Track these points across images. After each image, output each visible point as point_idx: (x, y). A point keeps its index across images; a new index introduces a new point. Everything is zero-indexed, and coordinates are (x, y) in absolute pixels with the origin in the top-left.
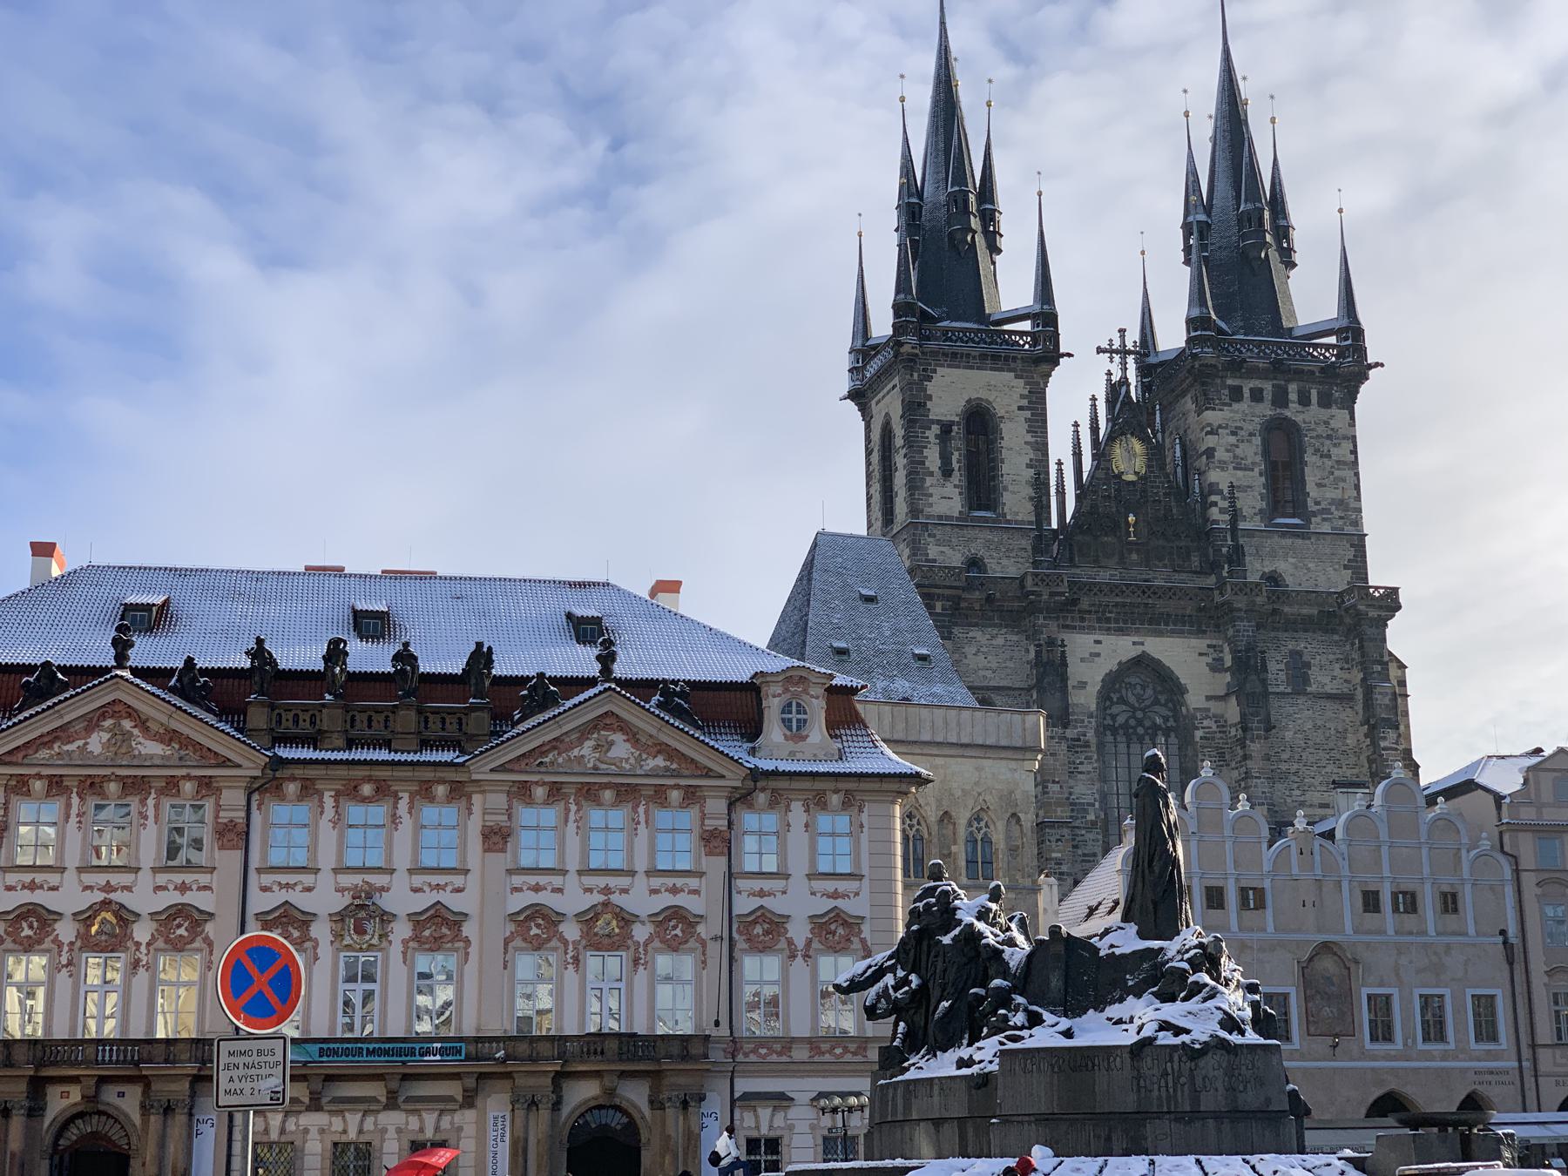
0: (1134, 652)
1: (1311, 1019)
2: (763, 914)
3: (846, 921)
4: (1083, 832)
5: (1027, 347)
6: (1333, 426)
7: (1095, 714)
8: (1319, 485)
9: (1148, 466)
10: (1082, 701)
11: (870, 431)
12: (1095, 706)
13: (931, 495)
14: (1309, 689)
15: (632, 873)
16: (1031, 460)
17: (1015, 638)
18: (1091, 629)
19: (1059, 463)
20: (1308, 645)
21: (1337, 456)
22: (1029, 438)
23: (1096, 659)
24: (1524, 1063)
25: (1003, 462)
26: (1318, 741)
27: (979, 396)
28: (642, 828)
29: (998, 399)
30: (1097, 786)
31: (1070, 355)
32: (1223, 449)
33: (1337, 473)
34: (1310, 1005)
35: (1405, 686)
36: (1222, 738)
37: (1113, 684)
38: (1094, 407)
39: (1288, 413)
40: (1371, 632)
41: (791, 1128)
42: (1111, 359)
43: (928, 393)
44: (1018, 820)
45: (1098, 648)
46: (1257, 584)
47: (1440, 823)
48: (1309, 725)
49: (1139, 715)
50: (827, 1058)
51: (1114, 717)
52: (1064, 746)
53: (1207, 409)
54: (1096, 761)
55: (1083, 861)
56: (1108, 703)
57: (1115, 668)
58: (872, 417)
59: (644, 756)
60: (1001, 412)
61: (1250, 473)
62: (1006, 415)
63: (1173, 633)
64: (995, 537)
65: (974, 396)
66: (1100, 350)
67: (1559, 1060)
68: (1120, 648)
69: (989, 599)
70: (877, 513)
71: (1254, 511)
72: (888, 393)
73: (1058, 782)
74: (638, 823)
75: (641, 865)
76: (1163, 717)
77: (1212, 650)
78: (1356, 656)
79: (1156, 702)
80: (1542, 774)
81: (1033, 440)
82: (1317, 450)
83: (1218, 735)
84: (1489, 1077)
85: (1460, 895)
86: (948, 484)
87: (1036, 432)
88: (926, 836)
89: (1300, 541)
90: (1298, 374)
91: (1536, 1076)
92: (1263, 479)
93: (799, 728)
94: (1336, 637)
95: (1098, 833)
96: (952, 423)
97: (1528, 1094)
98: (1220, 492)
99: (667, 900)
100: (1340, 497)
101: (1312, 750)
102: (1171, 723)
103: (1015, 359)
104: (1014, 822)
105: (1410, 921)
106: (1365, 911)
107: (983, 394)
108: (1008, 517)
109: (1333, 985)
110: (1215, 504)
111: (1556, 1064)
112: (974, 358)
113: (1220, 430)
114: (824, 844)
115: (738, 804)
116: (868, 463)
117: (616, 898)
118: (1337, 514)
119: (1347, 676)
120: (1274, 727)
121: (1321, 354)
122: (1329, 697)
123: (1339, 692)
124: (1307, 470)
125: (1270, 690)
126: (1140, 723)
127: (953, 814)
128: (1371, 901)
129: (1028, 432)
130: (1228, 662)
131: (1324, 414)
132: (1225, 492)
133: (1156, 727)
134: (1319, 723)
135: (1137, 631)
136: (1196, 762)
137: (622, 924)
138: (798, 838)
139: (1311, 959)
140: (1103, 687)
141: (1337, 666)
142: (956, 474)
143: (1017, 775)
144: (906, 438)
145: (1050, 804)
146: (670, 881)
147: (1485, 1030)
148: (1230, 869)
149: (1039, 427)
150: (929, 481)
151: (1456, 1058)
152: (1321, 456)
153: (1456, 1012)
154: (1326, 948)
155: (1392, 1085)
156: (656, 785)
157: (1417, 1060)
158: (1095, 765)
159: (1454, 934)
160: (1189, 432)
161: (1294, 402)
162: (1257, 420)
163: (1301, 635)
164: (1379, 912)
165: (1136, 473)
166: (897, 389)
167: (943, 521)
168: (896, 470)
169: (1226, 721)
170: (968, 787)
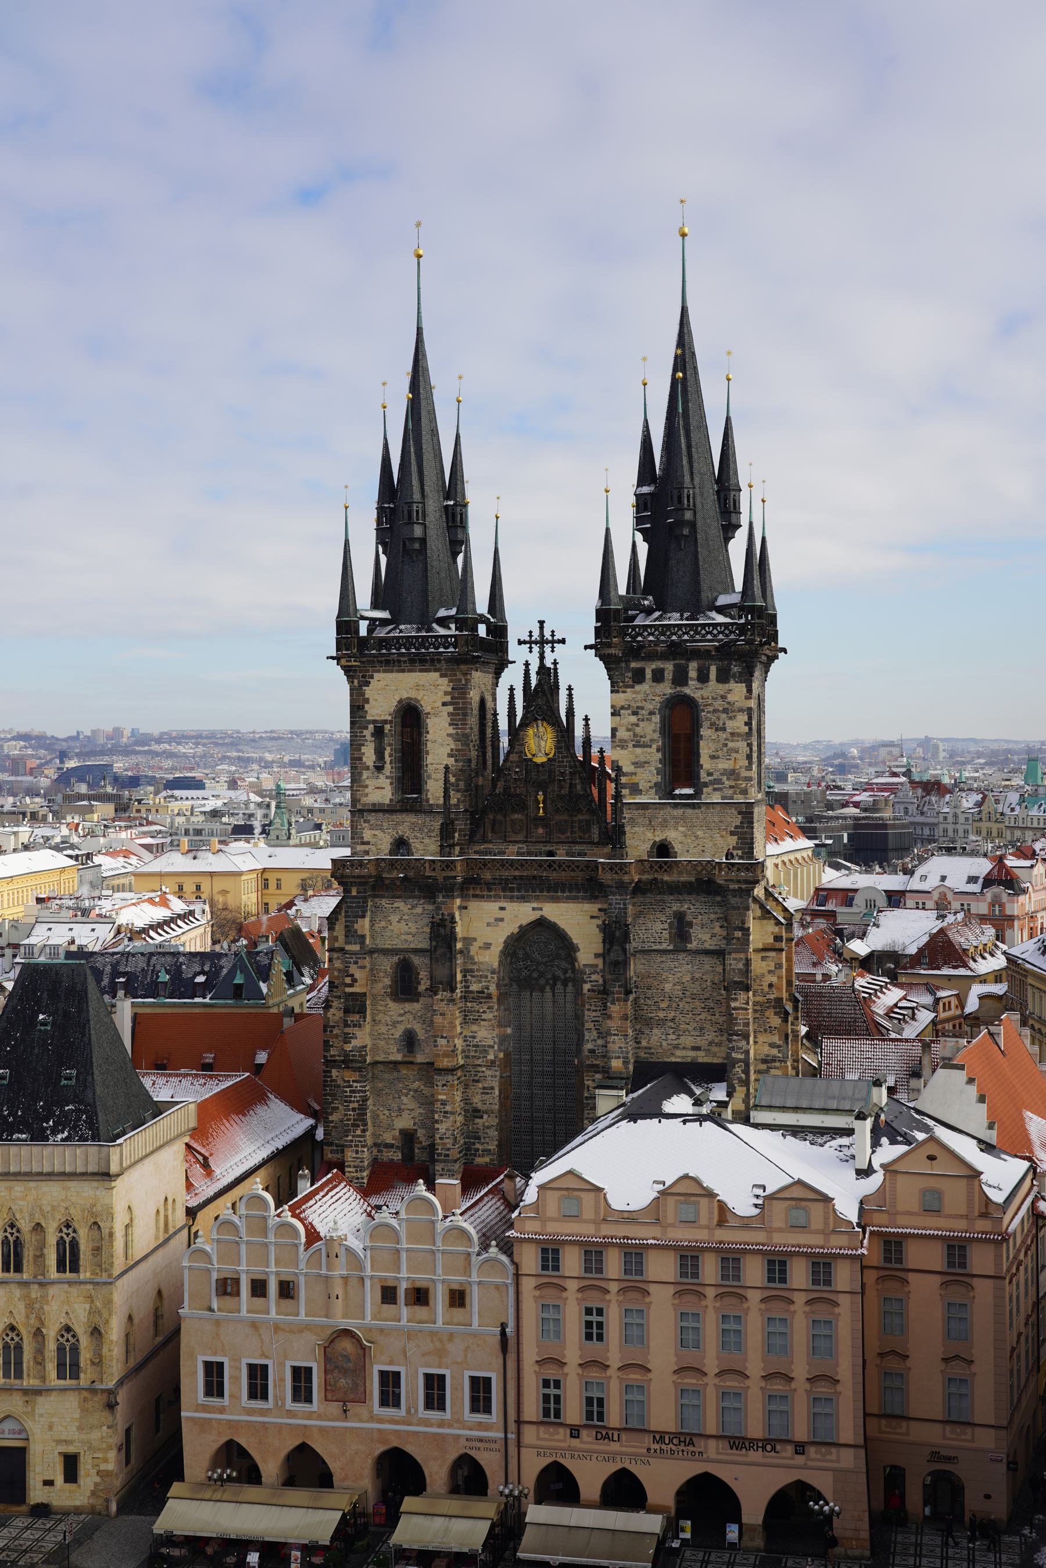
0: (534, 916)
1: (329, 1388)
4: (484, 1069)
8: (713, 757)
10: (487, 959)
13: (367, 786)
14: (689, 946)
16: (452, 750)
18: (497, 898)
20: (690, 907)
22: (451, 730)
23: (500, 923)
24: (509, 1436)
25: (427, 753)
26: (695, 991)
30: (497, 1031)
32: (624, 728)
33: (731, 745)
39: (687, 691)
42: (531, 648)
44: (99, 1227)
48: (688, 978)
57: (516, 930)
60: (427, 709)
61: (648, 750)
62: (432, 712)
63: (568, 899)
65: (405, 696)
67: (542, 1435)
71: (649, 784)
80: (549, 1193)
81: (454, 732)
82: (713, 724)
84: (479, 1444)
85: (467, 1292)
86: (381, 776)
90: (697, 654)
91: (519, 1447)
92: (659, 755)
96: (385, 722)
97: (509, 1460)
101: (689, 1000)
102: (569, 974)
103: (439, 661)
105: (421, 1311)
106: (383, 1303)
107: (413, 694)
108: (431, 802)
111: (539, 1438)
112: (405, 662)
113: (622, 712)
118: (727, 783)
122: (707, 952)
123: (718, 948)
127: (43, 1224)
128: (389, 1295)
129: (450, 725)
131: (721, 688)
133: (555, 979)
134: (697, 975)
135: (537, 899)
136: (583, 1011)
139: (332, 1341)
142: (388, 766)
143: (98, 1193)
149: (460, 720)
150: (365, 774)
151: (450, 1426)
152: (717, 730)
153: (454, 1388)
154: (347, 1333)
155: (395, 1443)
157: (417, 1425)
162: (657, 699)
163: (686, 897)
164: (396, 1303)
167: (377, 809)
170: (55, 1204)
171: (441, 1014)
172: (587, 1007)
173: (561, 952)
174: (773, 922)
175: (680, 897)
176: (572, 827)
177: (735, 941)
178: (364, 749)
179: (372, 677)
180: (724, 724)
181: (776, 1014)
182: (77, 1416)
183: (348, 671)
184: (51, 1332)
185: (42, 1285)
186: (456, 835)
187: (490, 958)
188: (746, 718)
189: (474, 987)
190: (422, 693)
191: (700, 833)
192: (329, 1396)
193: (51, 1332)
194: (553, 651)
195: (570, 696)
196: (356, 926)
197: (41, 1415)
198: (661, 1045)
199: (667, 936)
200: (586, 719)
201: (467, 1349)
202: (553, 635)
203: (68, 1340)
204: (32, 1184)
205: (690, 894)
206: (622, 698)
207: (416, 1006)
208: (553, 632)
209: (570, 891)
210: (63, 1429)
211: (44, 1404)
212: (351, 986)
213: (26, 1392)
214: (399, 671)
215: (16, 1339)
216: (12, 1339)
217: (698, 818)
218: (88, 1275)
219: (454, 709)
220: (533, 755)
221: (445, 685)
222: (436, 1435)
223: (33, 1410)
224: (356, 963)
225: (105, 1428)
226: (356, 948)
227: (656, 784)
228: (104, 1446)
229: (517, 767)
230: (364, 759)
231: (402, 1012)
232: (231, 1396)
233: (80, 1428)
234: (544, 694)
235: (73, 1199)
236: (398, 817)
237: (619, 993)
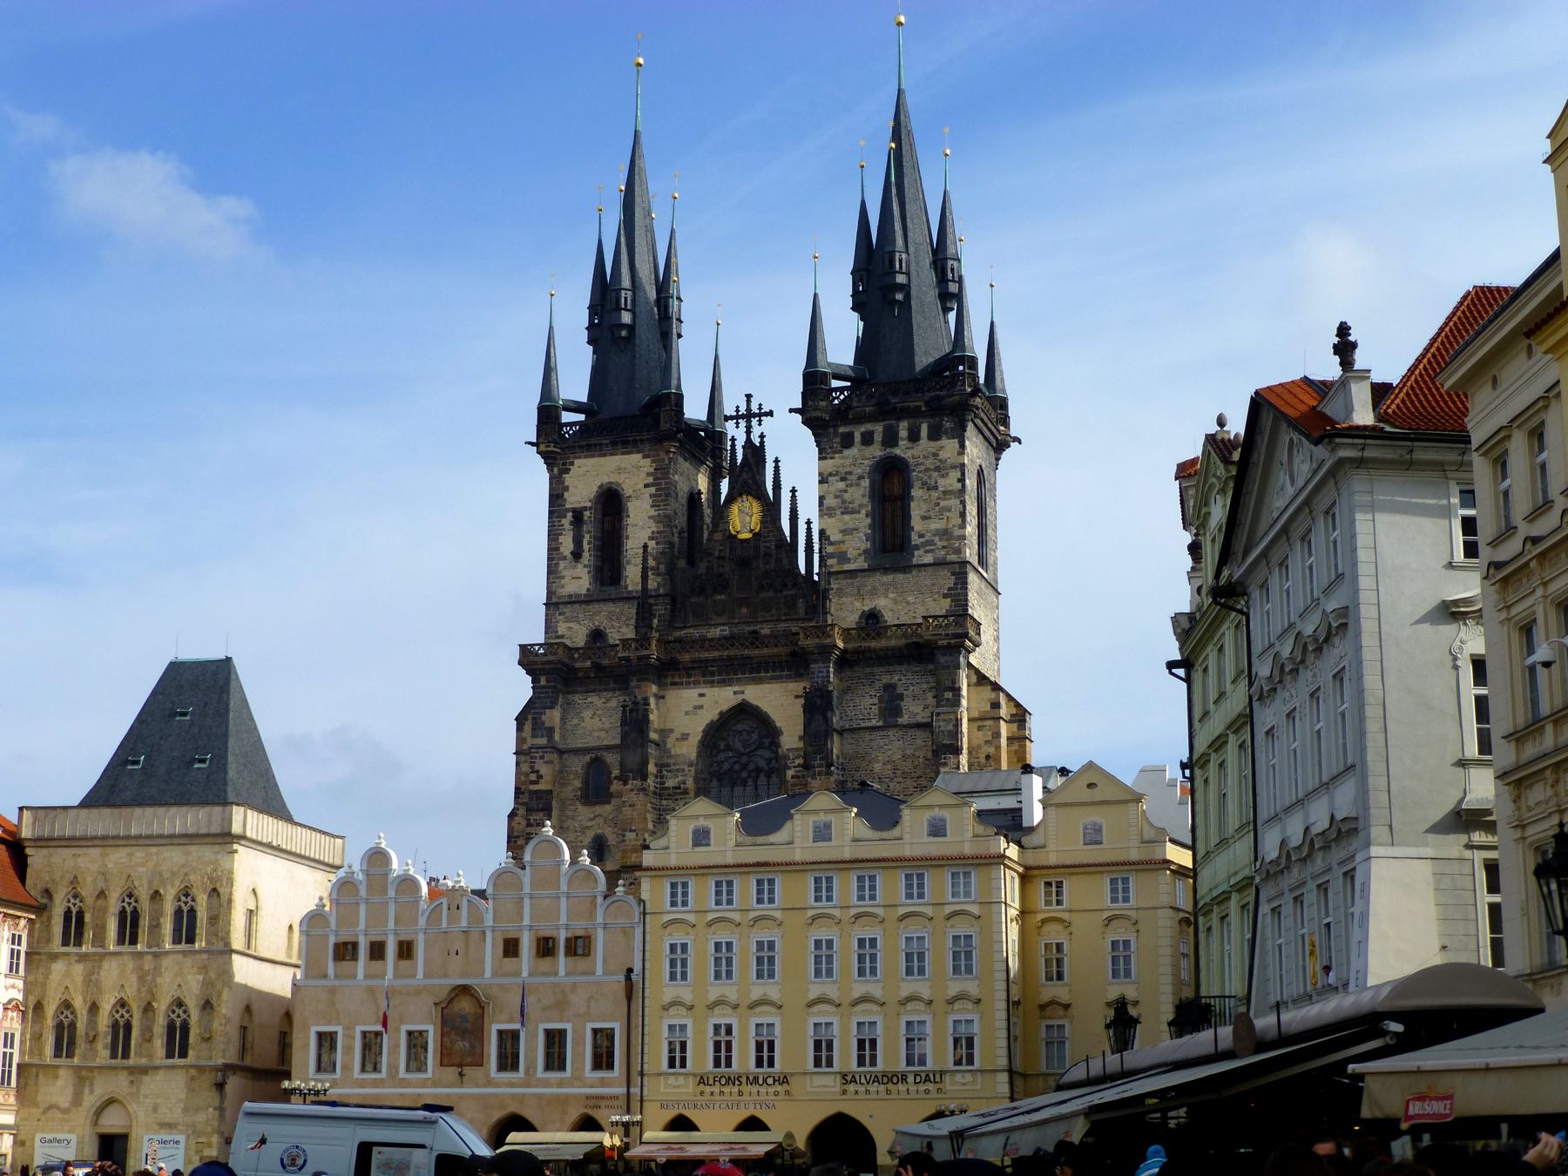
1: (444, 1051)
6: (941, 457)
8: (924, 518)
9: (763, 522)
10: (684, 751)
12: (695, 755)
13: (563, 577)
14: (900, 721)
16: (653, 532)
18: (697, 683)
21: (944, 486)
22: (653, 512)
25: (627, 538)
26: (907, 770)
32: (832, 496)
33: (943, 503)
34: (445, 1040)
37: (716, 733)
39: (897, 451)
42: (737, 423)
43: (566, 484)
45: (702, 701)
47: (578, 874)
57: (717, 717)
61: (857, 516)
65: (606, 480)
68: (721, 698)
69: (597, 667)
81: (656, 513)
85: (593, 937)
86: (580, 566)
89: (900, 576)
92: (869, 520)
96: (585, 508)
100: (944, 527)
101: (900, 779)
104: (215, 895)
107: (614, 478)
108: (630, 589)
109: (467, 1022)
112: (607, 444)
118: (940, 544)
122: (919, 726)
124: (913, 505)
128: (511, 948)
129: (652, 506)
133: (758, 770)
134: (909, 752)
135: (739, 681)
142: (586, 555)
147: (603, 1060)
148: (391, 925)
150: (562, 564)
152: (929, 489)
153: (576, 1044)
154: (464, 990)
157: (536, 1086)
159: (585, 973)
161: (903, 439)
162: (866, 462)
163: (897, 668)
167: (574, 601)
170: (175, 869)
171: (630, 806)
173: (764, 740)
174: (989, 688)
175: (891, 668)
178: (561, 539)
179: (572, 464)
180: (936, 482)
182: (183, 1096)
183: (549, 459)
184: (161, 1006)
185: (156, 955)
186: (655, 621)
187: (688, 750)
188: (959, 475)
189: (670, 783)
190: (623, 476)
191: (910, 598)
193: (161, 1006)
194: (760, 425)
195: (777, 469)
196: (544, 718)
197: (146, 1097)
200: (793, 491)
201: (591, 998)
202: (760, 409)
203: (179, 1016)
204: (153, 850)
205: (900, 664)
206: (830, 464)
207: (608, 808)
208: (760, 405)
209: (774, 671)
210: (167, 1111)
211: (153, 1084)
212: (536, 782)
213: (132, 1070)
214: (600, 456)
215: (126, 1016)
216: (122, 1016)
217: (909, 583)
218: (203, 943)
219: (657, 490)
220: (738, 532)
221: (646, 465)
222: (557, 1096)
223: (138, 1091)
224: (542, 757)
225: (211, 1110)
226: (543, 741)
228: (209, 1129)
229: (721, 545)
230: (562, 549)
231: (592, 816)
232: (343, 1068)
233: (185, 1110)
234: (750, 469)
235: (194, 864)
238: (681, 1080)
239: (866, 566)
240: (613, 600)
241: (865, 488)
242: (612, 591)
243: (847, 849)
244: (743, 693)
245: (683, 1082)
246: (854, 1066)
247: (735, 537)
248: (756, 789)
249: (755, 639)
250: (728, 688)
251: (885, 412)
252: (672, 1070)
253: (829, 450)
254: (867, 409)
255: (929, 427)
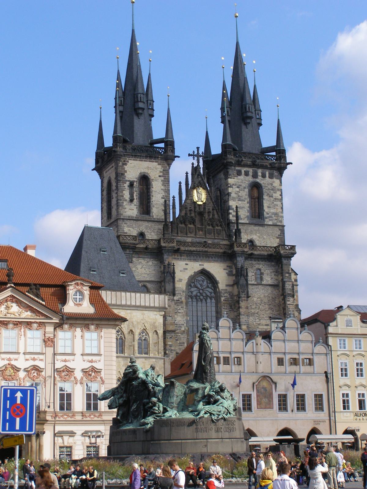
0: (200, 268)
2: (66, 368)
3: (95, 371)
4: (180, 335)
5: (163, 153)
7: (185, 291)
8: (269, 207)
9: (207, 199)
10: (180, 286)
11: (103, 183)
13: (126, 208)
15: (19, 353)
16: (163, 196)
17: (156, 262)
18: (184, 260)
19: (174, 197)
21: (275, 196)
22: (163, 187)
23: (186, 271)
25: (153, 196)
26: (266, 301)
27: (144, 171)
28: (23, 337)
29: (152, 173)
30: (185, 318)
31: (179, 157)
32: (234, 193)
33: (275, 203)
35: (297, 281)
36: (231, 300)
38: (187, 176)
39: (258, 180)
40: (285, 261)
41: (75, 443)
43: (125, 170)
45: (186, 267)
46: (245, 244)
49: (201, 291)
50: (88, 419)
51: (192, 292)
52: (173, 303)
53: (229, 178)
54: (185, 308)
55: (179, 345)
56: (190, 287)
57: (193, 274)
58: (104, 178)
59: (23, 311)
61: (244, 202)
64: (149, 224)
65: (143, 171)
66: (189, 155)
68: (195, 266)
70: (105, 214)
71: (245, 216)
72: (110, 169)
73: (171, 316)
74: (21, 335)
75: (22, 350)
76: (210, 292)
77: (228, 268)
78: (280, 270)
79: (208, 287)
81: (164, 188)
83: (230, 299)
87: (165, 185)
88: (124, 339)
89: (261, 228)
92: (248, 205)
93: (79, 301)
94: (273, 263)
95: (185, 335)
98: (233, 209)
99: (32, 363)
101: (264, 305)
104: (155, 333)
106: (279, 365)
107: (146, 171)
108: (154, 217)
110: (231, 213)
112: (143, 156)
114: (87, 343)
115: (57, 328)
116: (102, 195)
117: (13, 363)
119: (276, 277)
120: (250, 297)
121: (270, 159)
123: (273, 284)
124: (264, 201)
125: (249, 283)
126: (201, 294)
127: (133, 331)
128: (280, 362)
129: (162, 185)
130: (234, 272)
131: (270, 181)
132: (235, 209)
133: (207, 296)
135: (201, 260)
137: (15, 371)
138: (78, 341)
140: (188, 281)
141: (273, 274)
142: (135, 200)
143: (157, 317)
144: (117, 187)
145: (168, 324)
146: (33, 356)
149: (166, 183)
150: (125, 203)
152: (270, 197)
156: (28, 322)
158: (185, 310)
160: (222, 186)
161: (260, 176)
162: (247, 182)
163: (262, 263)
165: (202, 201)
166: (114, 168)
167: (130, 219)
168: (113, 198)
169: (233, 294)
170: (139, 321)
172: (223, 307)
173: (209, 285)
175: (259, 262)
176: (214, 232)
177: (286, 278)
178: (124, 192)
179: (128, 162)
180: (272, 194)
181: (296, 311)
188: (280, 193)
192: (259, 407)
198: (253, 324)
199: (254, 278)
204: (129, 311)
219: (164, 179)
221: (160, 168)
227: (247, 216)
229: (190, 205)
230: (124, 196)
235: (147, 319)
236: (140, 223)
237: (244, 297)
238: (348, 414)
239: (248, 222)
240: (148, 221)
241: (246, 192)
242: (147, 217)
243: (359, 330)
244: (203, 265)
245: (349, 415)
246: (358, 409)
247: (195, 203)
248: (206, 304)
249: (205, 244)
250: (198, 263)
251: (254, 165)
252: (345, 411)
253: (232, 175)
254: (248, 162)
255: (269, 173)
